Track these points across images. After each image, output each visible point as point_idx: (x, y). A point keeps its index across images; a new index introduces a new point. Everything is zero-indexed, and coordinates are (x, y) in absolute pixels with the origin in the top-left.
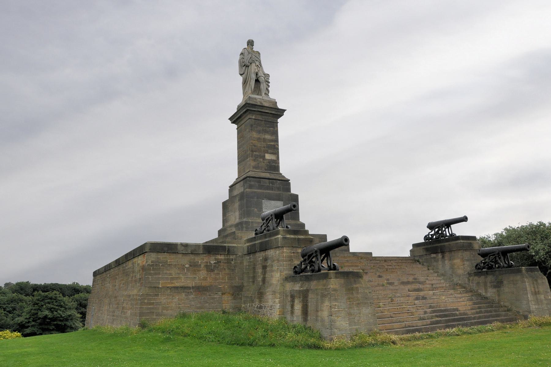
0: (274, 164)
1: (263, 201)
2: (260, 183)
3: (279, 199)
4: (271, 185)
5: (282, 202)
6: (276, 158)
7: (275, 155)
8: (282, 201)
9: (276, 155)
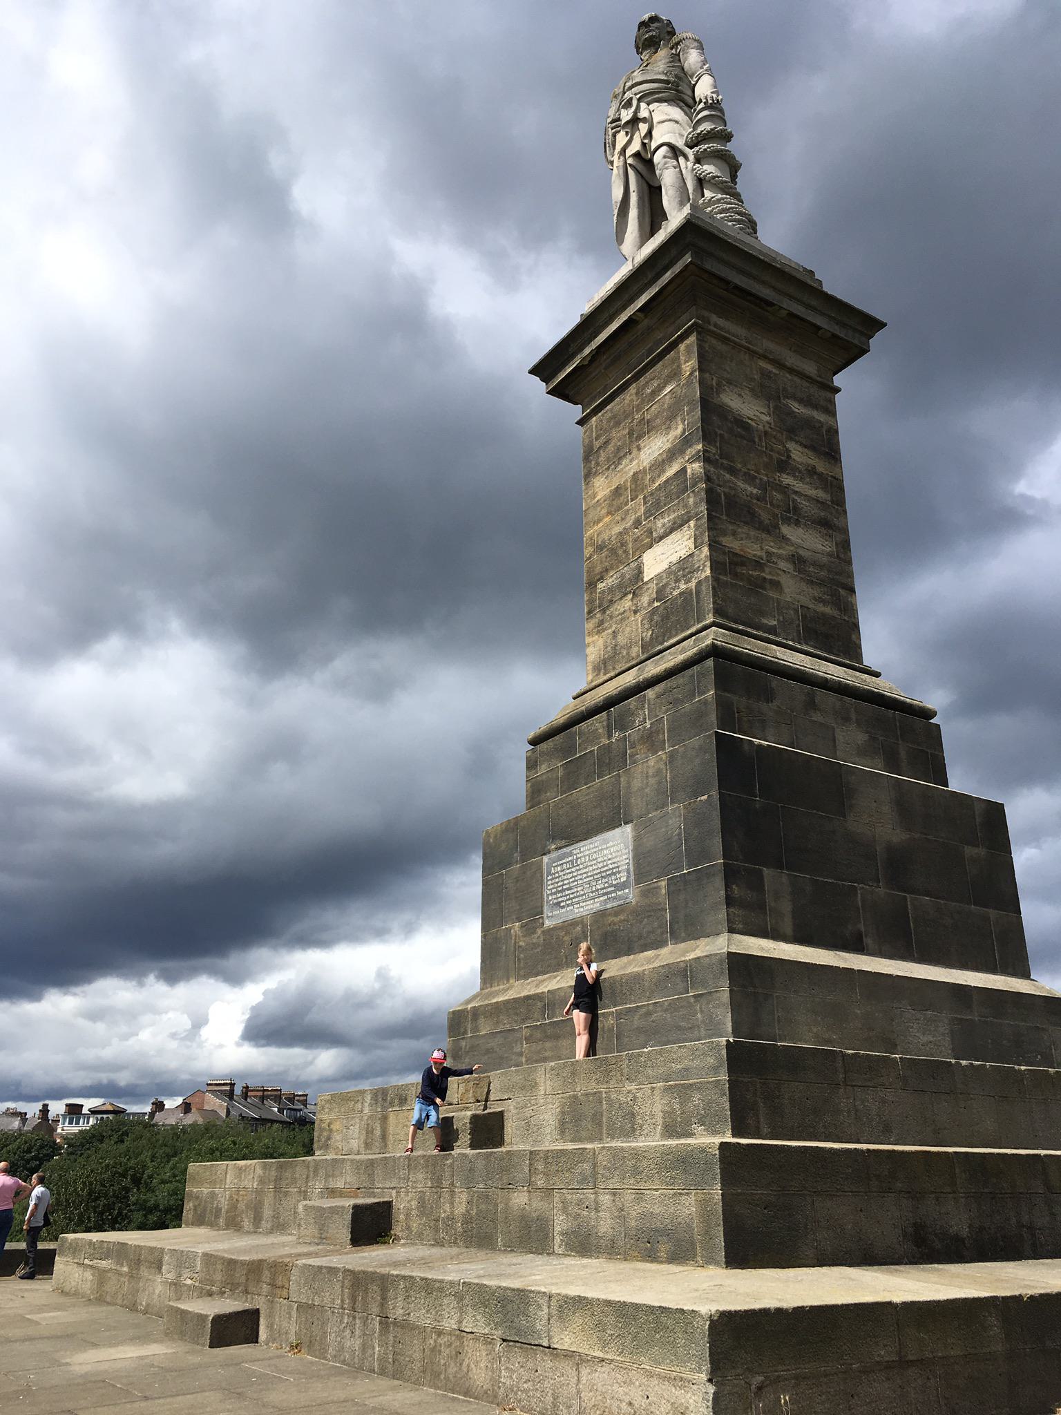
0: (683, 586)
1: (546, 859)
2: (570, 749)
3: (612, 823)
4: (616, 735)
5: (628, 829)
6: (691, 544)
7: (685, 528)
8: (626, 823)
9: (692, 523)
